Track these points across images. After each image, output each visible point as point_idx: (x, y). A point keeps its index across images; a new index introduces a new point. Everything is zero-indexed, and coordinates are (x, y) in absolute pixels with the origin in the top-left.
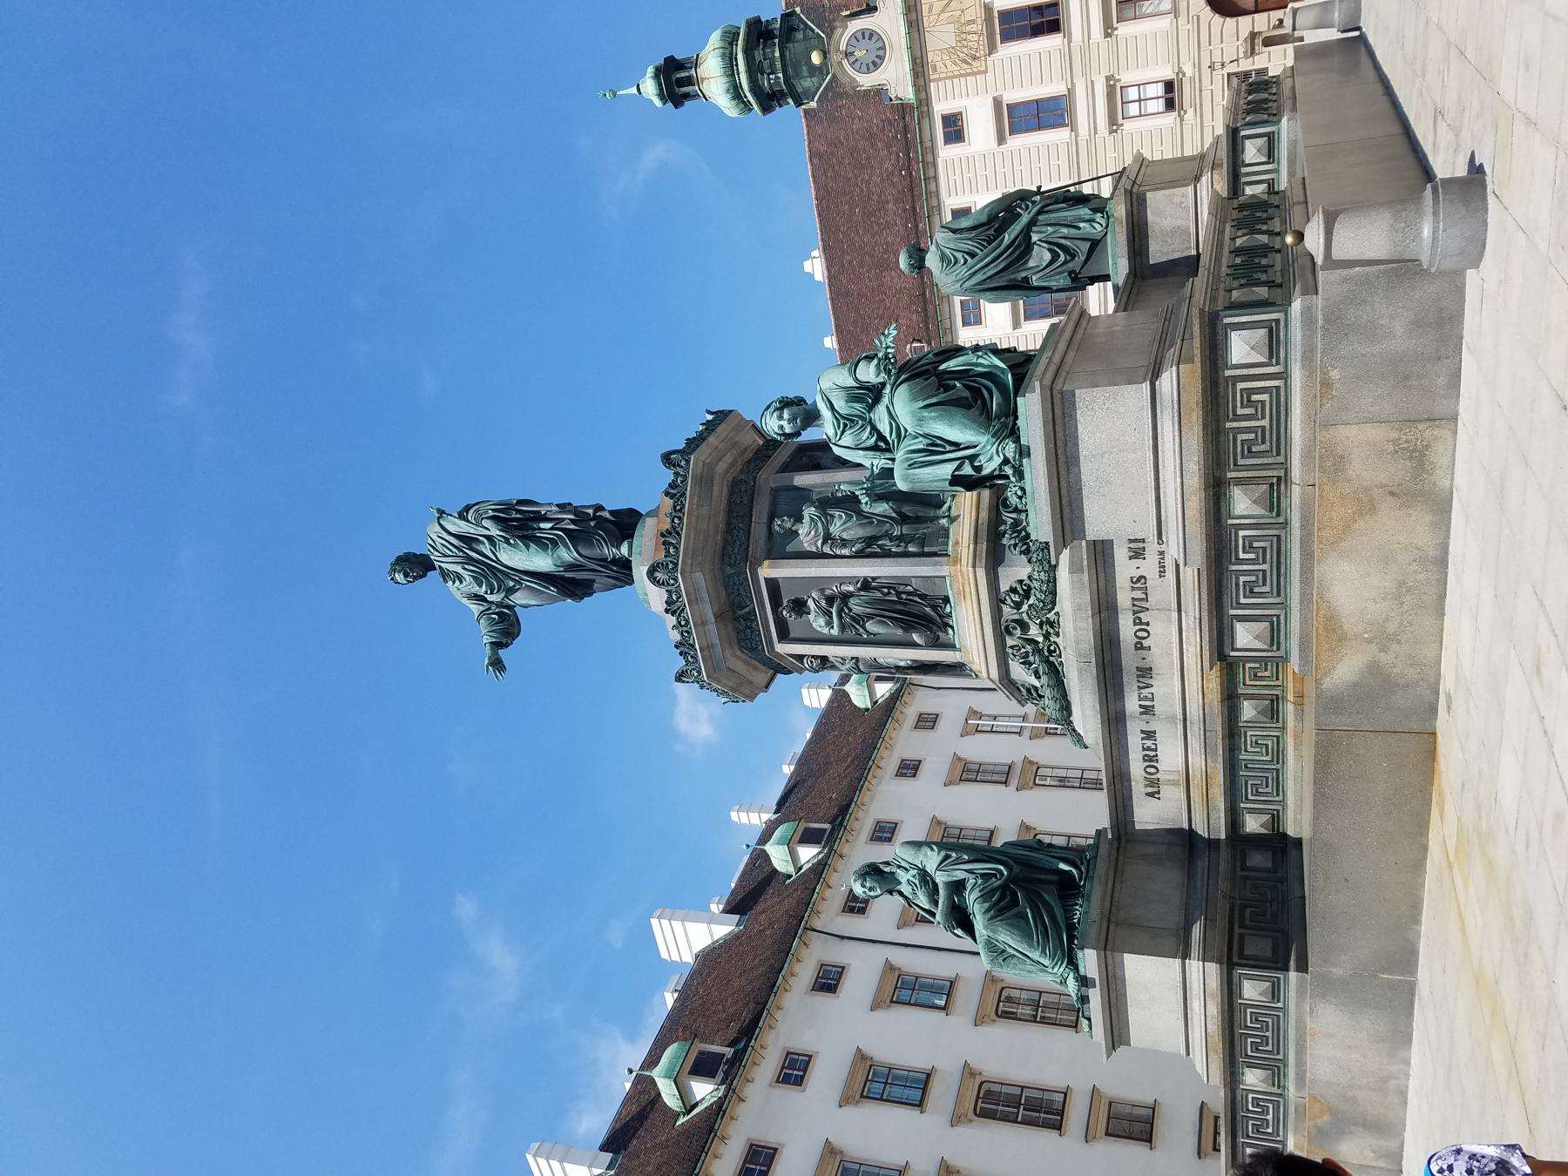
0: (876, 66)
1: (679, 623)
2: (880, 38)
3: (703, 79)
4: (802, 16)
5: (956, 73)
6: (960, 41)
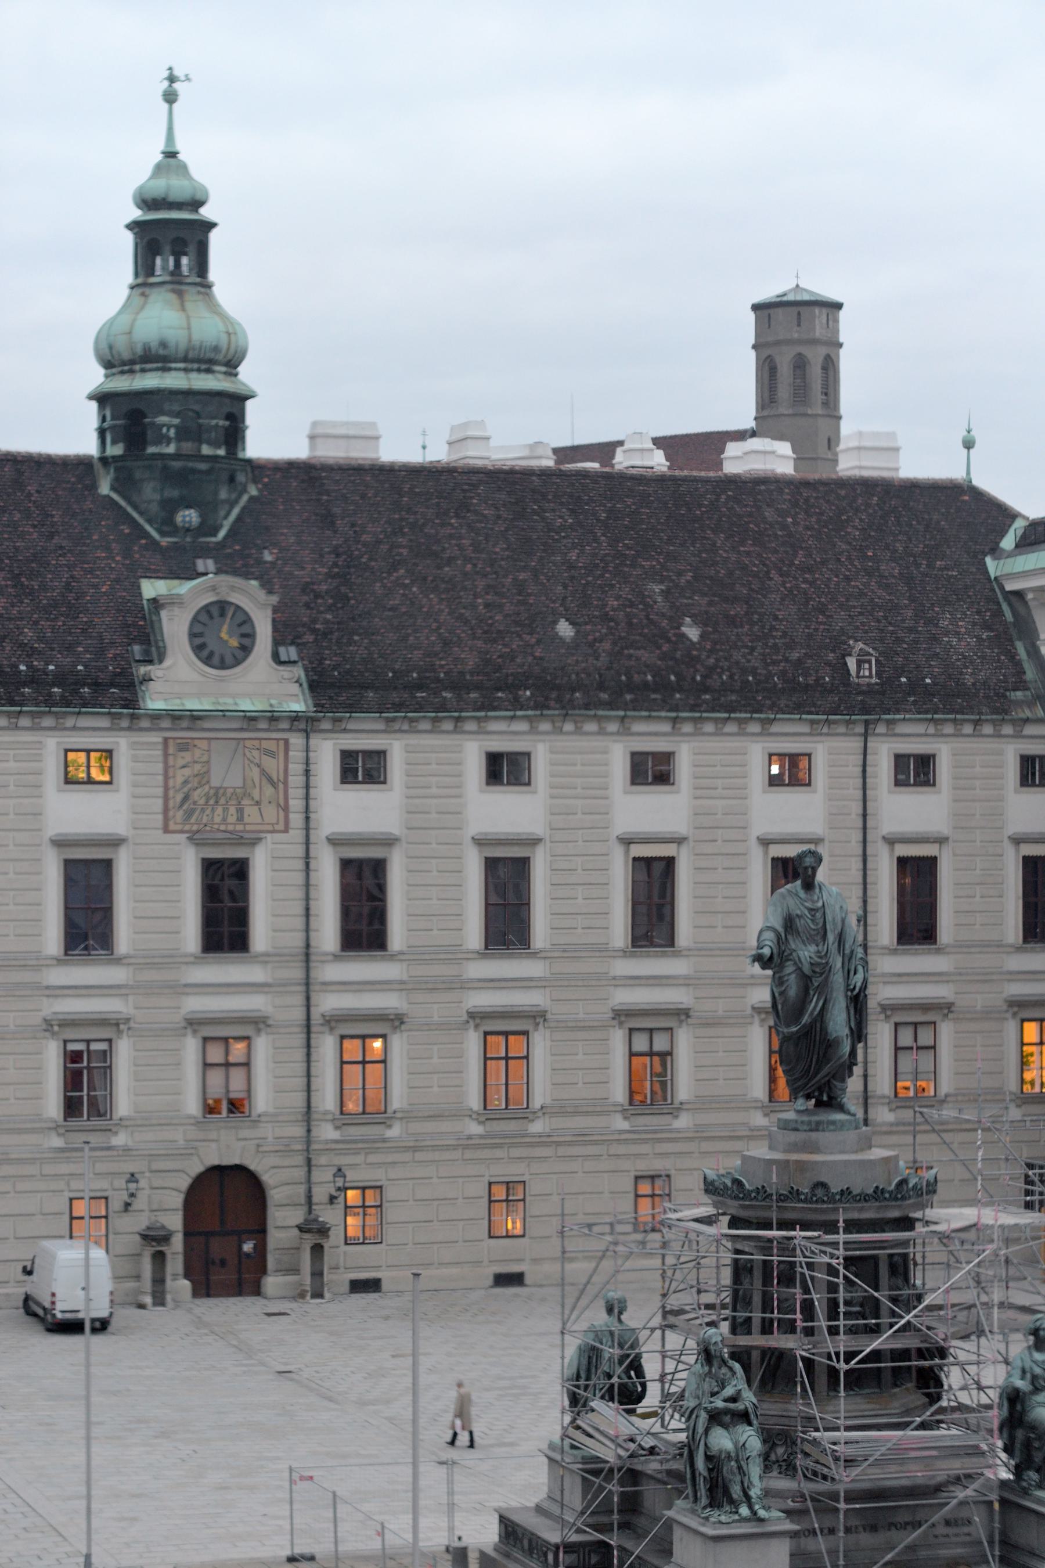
0: (198, 649)
1: (867, 1195)
2: (237, 662)
3: (180, 294)
4: (245, 498)
5: (171, 783)
6: (216, 794)
